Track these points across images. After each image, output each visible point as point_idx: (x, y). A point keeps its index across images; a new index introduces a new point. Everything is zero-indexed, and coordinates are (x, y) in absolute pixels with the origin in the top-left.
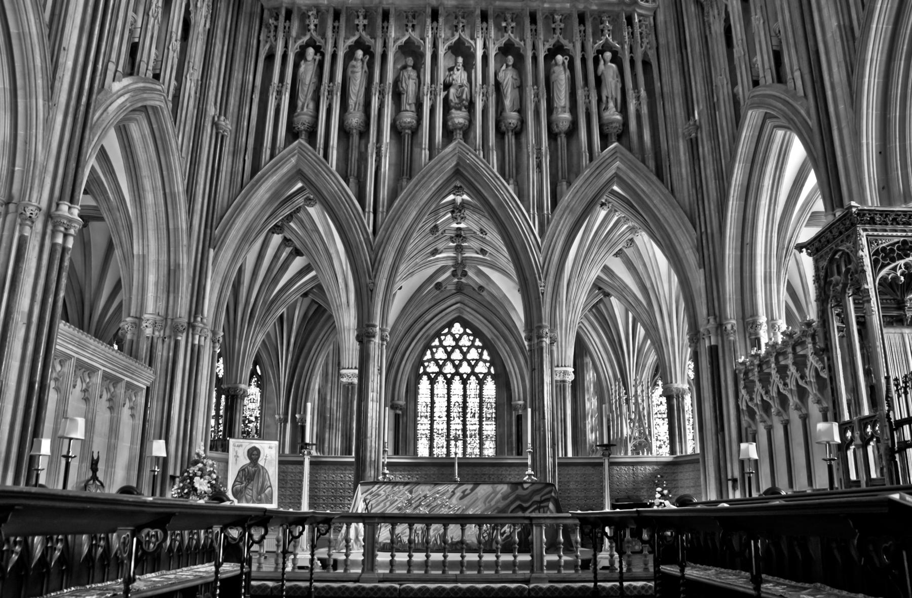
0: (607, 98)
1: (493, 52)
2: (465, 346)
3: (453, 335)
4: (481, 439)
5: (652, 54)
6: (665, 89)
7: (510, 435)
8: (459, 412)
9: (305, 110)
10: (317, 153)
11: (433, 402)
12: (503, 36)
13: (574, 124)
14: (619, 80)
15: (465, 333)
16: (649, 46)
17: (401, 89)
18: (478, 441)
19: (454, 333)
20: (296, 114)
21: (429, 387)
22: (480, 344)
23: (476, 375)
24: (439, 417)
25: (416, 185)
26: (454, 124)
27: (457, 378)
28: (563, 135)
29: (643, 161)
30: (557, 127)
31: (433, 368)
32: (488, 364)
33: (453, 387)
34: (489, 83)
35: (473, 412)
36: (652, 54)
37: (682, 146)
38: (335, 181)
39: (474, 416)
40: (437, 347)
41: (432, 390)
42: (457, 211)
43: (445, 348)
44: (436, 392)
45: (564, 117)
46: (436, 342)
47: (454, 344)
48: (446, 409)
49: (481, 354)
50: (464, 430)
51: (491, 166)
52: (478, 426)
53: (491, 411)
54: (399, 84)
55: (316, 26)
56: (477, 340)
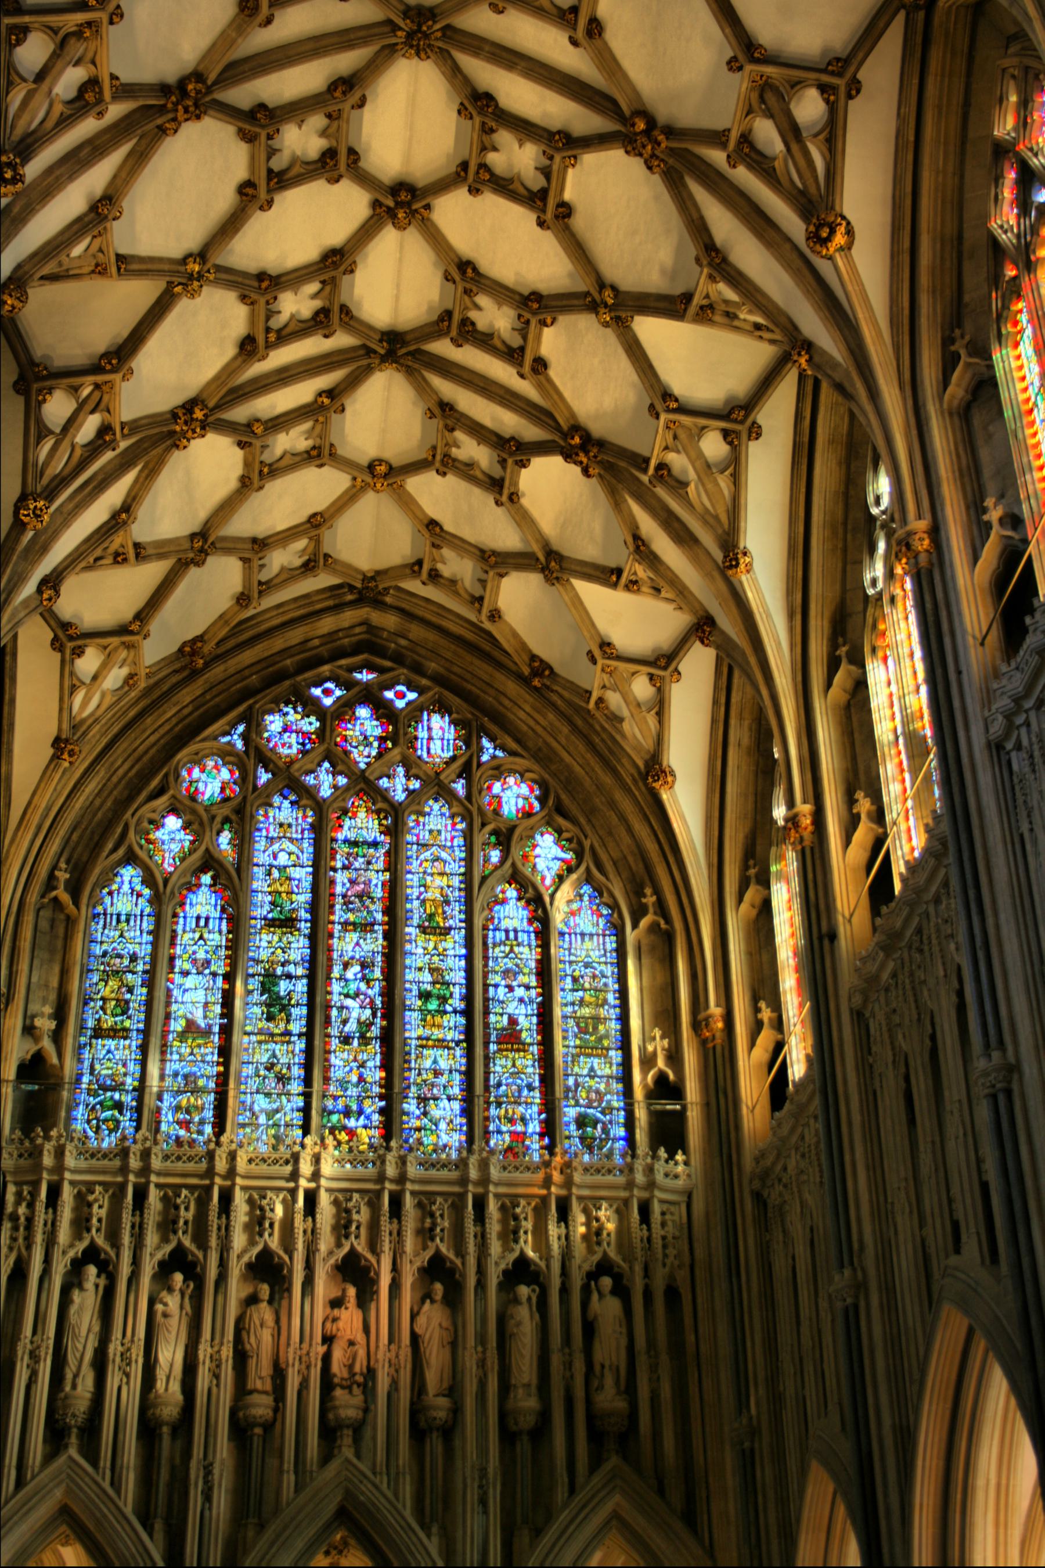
0: (603, 1366)
1: (408, 1279)
5: (682, 1276)
6: (703, 1348)
9: (79, 1388)
10: (99, 1479)
12: (425, 1248)
13: (545, 1415)
14: (624, 1330)
16: (677, 1263)
17: (248, 1347)
20: (62, 1395)
25: (273, 1544)
26: (337, 1418)
28: (525, 1438)
29: (661, 1491)
30: (516, 1423)
34: (400, 1341)
36: (682, 1276)
37: (729, 1460)
38: (132, 1534)
42: (334, 1552)
45: (527, 1403)
51: (400, 1506)
54: (244, 1334)
55: (100, 1220)
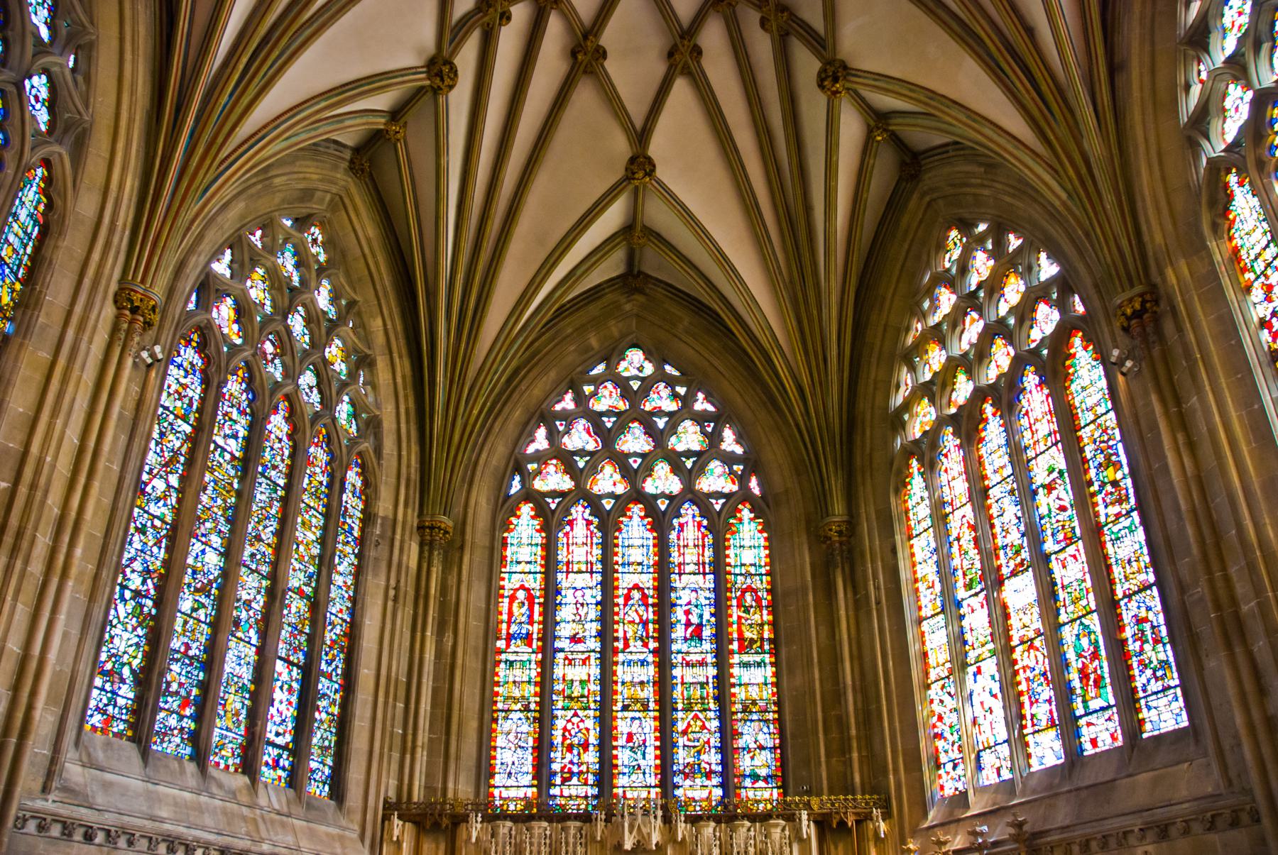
2: (659, 412)
3: (622, 384)
4: (724, 715)
7: (835, 696)
8: (645, 623)
11: (551, 591)
15: (659, 376)
18: (714, 724)
19: (626, 374)
21: (538, 538)
22: (711, 408)
23: (701, 501)
24: (574, 639)
27: (637, 510)
31: (554, 480)
32: (738, 468)
33: (621, 538)
35: (694, 619)
39: (697, 634)
40: (569, 418)
41: (549, 548)
43: (595, 419)
44: (562, 555)
46: (568, 403)
47: (622, 406)
48: (593, 613)
49: (714, 439)
50: (663, 684)
52: (712, 671)
53: (757, 618)
56: (700, 396)
